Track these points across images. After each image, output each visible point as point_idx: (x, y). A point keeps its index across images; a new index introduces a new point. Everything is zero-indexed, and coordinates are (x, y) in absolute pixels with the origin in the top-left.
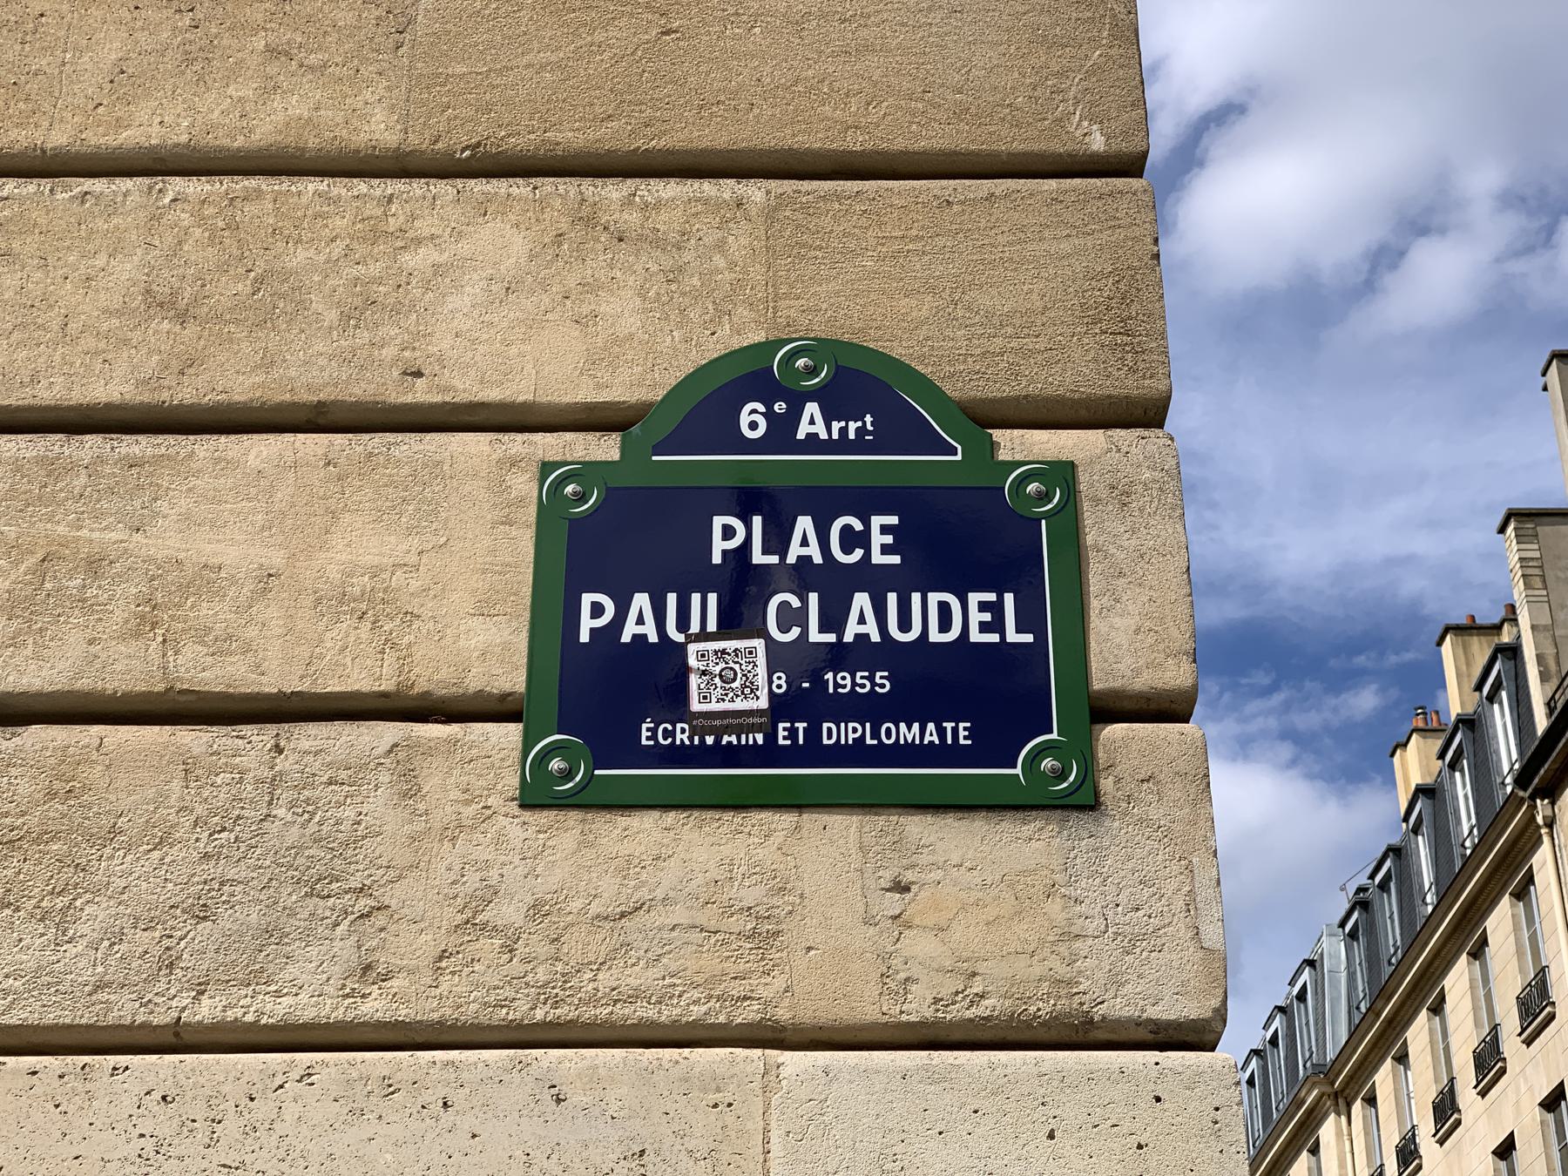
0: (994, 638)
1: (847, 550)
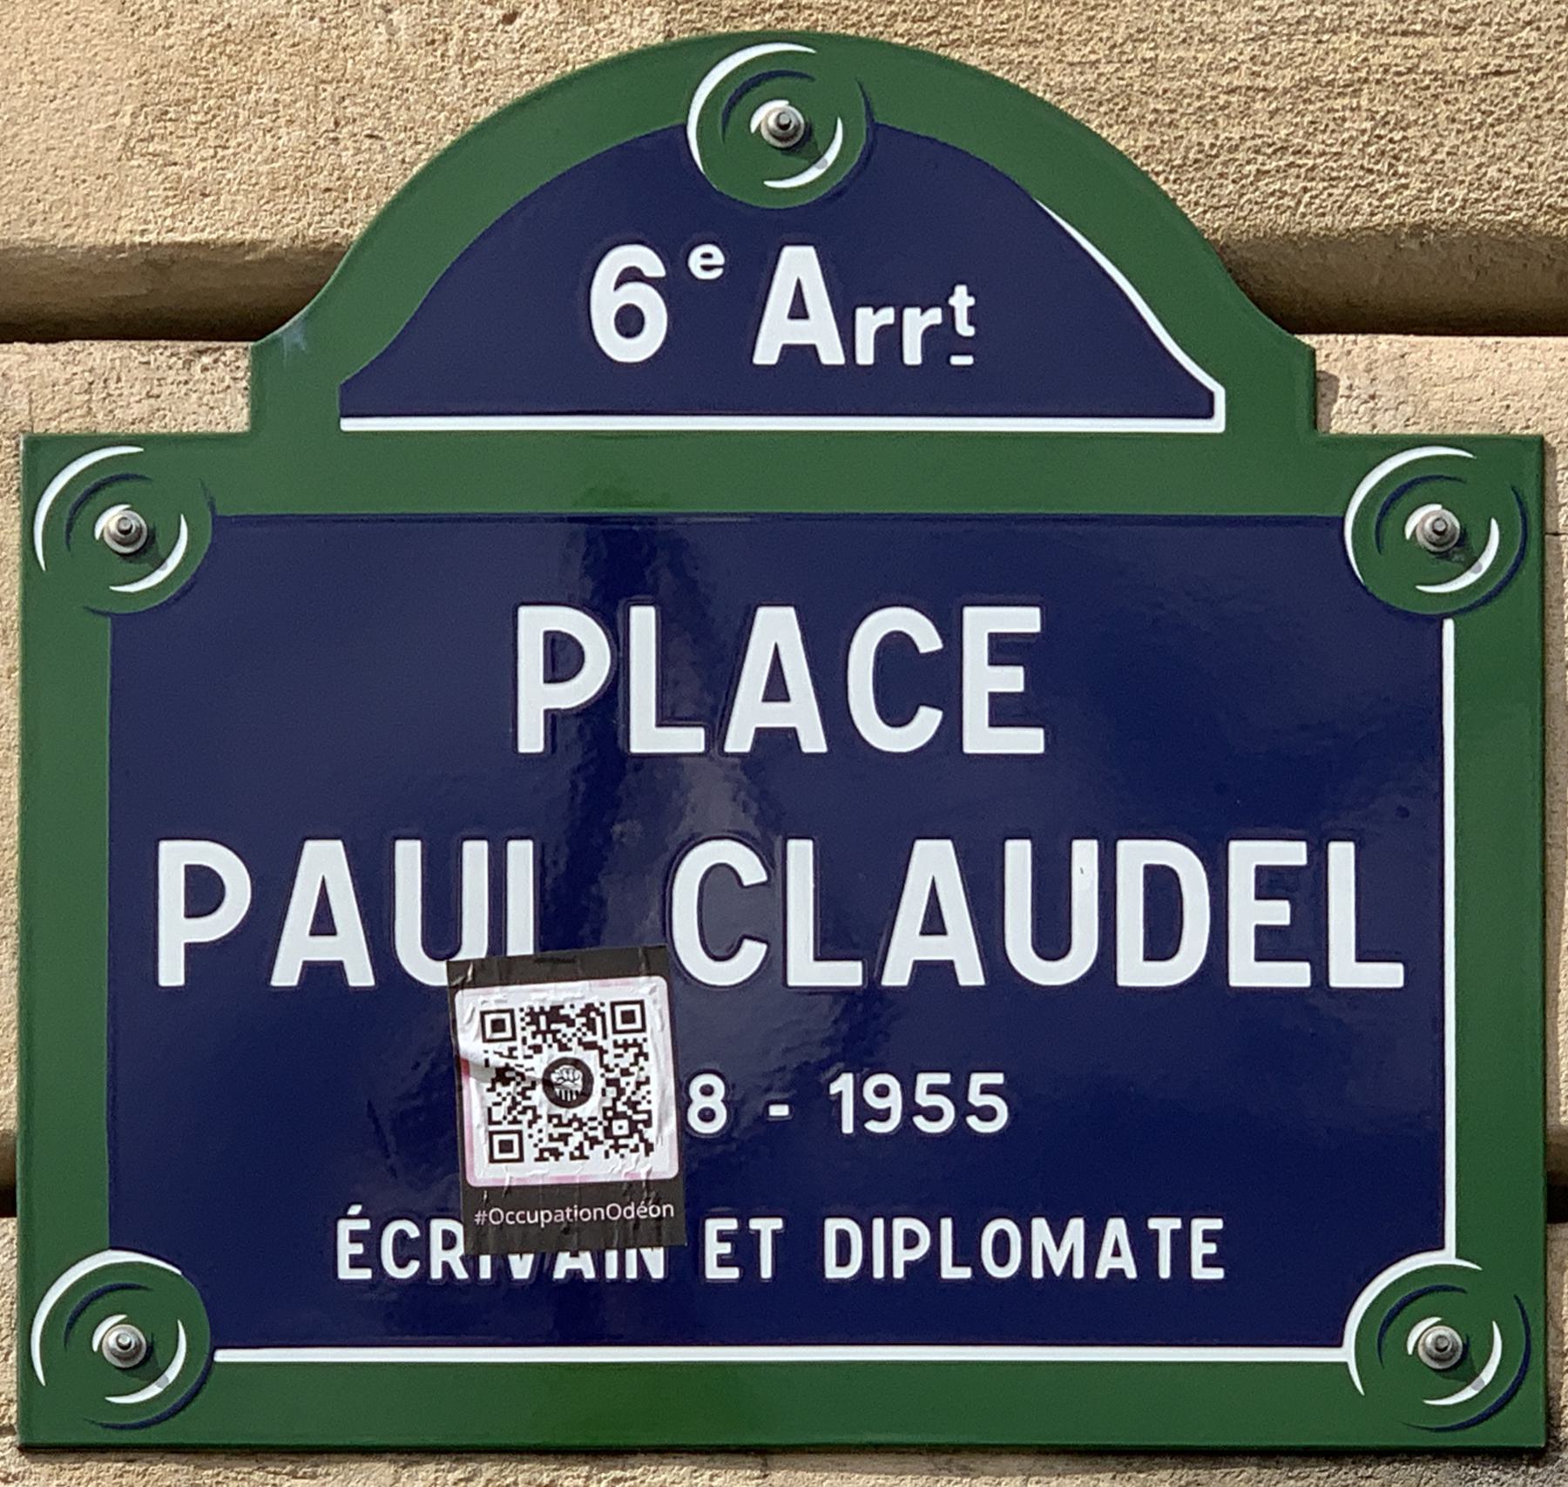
0: (1295, 975)
1: (895, 712)
